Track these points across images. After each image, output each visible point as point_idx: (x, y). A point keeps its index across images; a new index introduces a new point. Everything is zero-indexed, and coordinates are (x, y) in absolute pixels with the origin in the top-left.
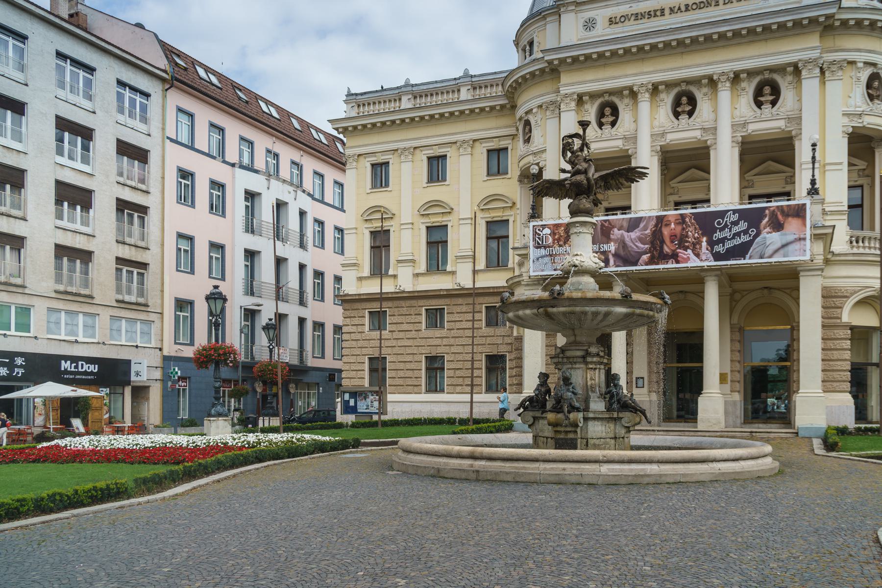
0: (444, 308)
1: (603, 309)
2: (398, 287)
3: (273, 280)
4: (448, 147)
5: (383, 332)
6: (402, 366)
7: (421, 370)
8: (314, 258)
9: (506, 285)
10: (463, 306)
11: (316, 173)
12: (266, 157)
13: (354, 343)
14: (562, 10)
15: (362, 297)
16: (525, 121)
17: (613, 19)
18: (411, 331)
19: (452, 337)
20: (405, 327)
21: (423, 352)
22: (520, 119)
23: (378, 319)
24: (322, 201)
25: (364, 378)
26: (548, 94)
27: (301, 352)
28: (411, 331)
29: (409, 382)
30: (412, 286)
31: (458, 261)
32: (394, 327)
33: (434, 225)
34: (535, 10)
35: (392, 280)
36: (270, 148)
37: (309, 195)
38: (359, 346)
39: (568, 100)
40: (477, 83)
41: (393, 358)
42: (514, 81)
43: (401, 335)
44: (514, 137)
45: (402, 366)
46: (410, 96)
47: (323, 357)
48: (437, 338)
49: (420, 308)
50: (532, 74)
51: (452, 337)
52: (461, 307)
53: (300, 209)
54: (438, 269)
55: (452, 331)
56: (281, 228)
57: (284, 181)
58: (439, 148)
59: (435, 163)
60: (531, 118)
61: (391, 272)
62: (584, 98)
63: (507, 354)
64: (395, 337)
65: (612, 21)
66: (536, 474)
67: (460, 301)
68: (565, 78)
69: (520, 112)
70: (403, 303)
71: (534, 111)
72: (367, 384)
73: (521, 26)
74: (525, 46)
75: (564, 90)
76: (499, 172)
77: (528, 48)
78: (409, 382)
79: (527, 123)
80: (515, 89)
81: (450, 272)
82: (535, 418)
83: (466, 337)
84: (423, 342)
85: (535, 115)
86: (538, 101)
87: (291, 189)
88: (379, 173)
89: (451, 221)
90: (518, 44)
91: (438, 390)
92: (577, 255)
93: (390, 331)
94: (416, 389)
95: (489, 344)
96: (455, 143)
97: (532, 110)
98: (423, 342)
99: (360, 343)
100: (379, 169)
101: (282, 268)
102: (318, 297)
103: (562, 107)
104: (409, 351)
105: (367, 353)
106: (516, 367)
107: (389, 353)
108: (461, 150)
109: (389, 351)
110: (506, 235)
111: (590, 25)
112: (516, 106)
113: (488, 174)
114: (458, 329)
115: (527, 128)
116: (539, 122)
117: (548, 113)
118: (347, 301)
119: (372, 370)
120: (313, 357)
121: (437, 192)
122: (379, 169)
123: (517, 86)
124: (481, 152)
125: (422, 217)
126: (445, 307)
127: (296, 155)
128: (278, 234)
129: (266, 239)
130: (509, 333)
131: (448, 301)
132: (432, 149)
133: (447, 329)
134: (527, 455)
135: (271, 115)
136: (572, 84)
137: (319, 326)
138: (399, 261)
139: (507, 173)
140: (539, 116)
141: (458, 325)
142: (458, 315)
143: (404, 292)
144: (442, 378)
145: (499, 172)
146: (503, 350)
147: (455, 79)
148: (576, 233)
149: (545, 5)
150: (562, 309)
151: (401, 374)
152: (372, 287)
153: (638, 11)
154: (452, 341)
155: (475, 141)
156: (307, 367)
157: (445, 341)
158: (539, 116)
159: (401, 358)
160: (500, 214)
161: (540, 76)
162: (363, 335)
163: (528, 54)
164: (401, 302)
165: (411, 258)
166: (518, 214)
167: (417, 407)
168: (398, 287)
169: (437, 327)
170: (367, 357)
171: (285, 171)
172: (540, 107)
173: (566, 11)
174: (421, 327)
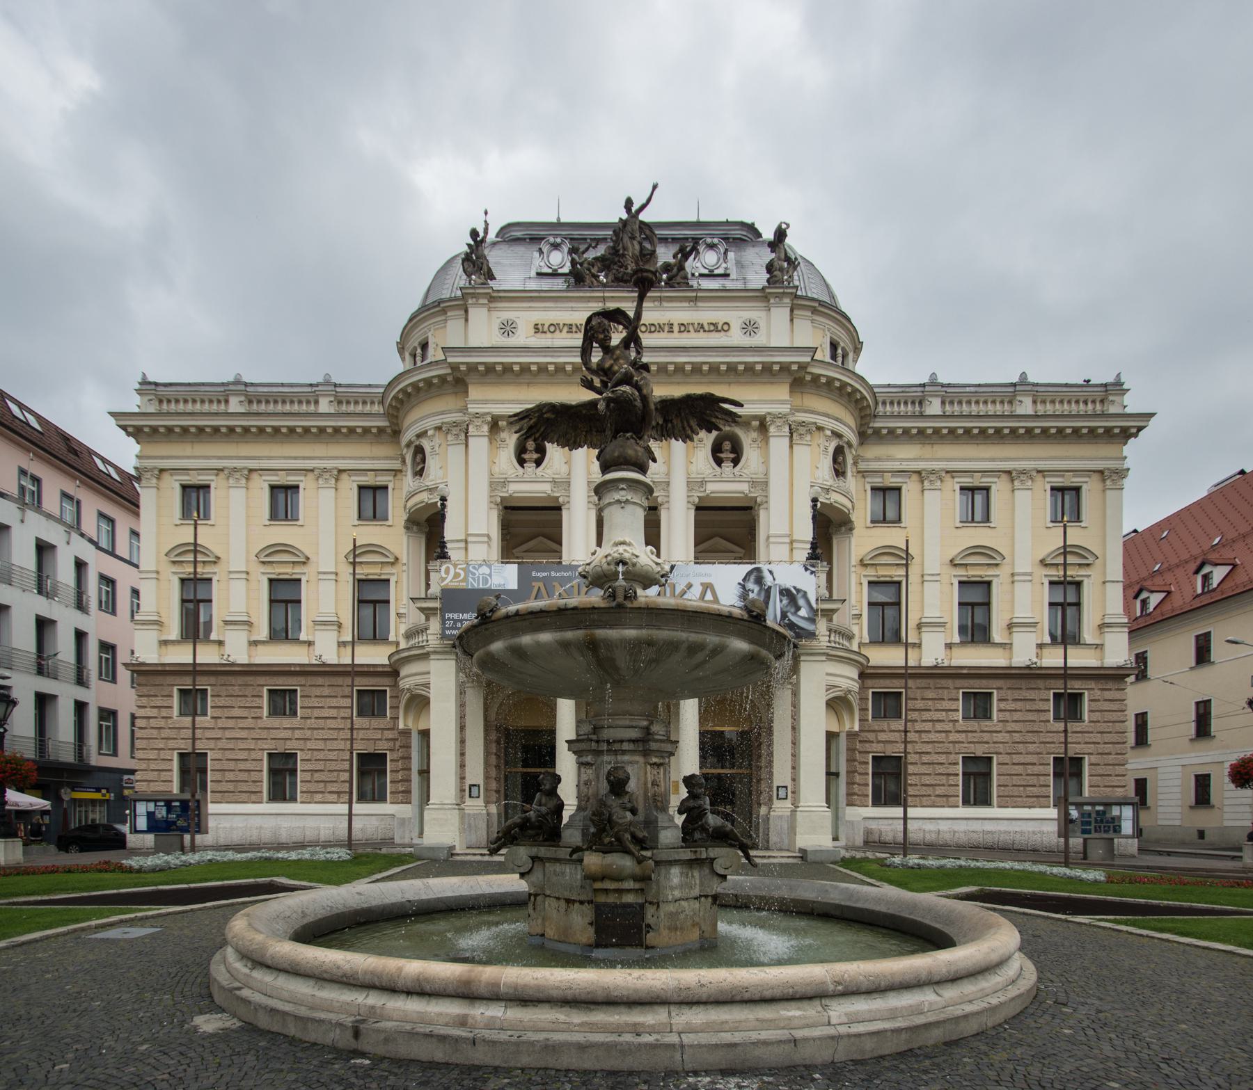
0: (296, 690)
1: (712, 639)
2: (226, 657)
3: (32, 647)
4: (301, 475)
5: (198, 719)
6: (231, 765)
7: (261, 771)
8: (98, 625)
9: (388, 663)
10: (323, 686)
11: (101, 515)
12: (19, 480)
13: (155, 732)
14: (470, 301)
15: (167, 668)
16: (416, 446)
17: (540, 327)
18: (246, 718)
19: (309, 729)
20: (236, 712)
21: (266, 747)
22: (408, 445)
23: (192, 700)
24: (112, 554)
25: (171, 781)
26: (450, 412)
27: (80, 746)
28: (246, 718)
29: (244, 787)
30: (246, 657)
31: (317, 627)
32: (218, 713)
33: (281, 577)
34: (428, 302)
35: (215, 647)
36: (25, 467)
37: (91, 541)
38: (163, 736)
39: (478, 422)
40: (343, 395)
41: (218, 755)
42: (401, 390)
43: (231, 723)
44: (396, 472)
45: (231, 765)
46: (242, 398)
47: (115, 754)
48: (285, 729)
49: (260, 688)
50: (428, 382)
51: (309, 729)
52: (322, 689)
53: (76, 557)
54: (287, 638)
55: (309, 721)
56: (45, 578)
57: (49, 516)
58: (287, 475)
59: (281, 497)
60: (425, 443)
61: (213, 636)
62: (500, 423)
63: (388, 752)
64: (220, 725)
65: (537, 329)
66: (671, 1046)
67: (320, 680)
68: (475, 392)
69: (408, 436)
70: (232, 679)
71: (430, 433)
72: (176, 790)
73: (411, 320)
74: (415, 348)
75: (473, 408)
76: (375, 516)
77: (419, 351)
78: (244, 787)
79: (420, 451)
80: (398, 409)
81: (305, 642)
82: (534, 859)
83: (329, 729)
84: (264, 734)
85: (431, 438)
86: (436, 421)
87: (61, 529)
88: (194, 503)
89: (307, 576)
90: (403, 348)
91: (288, 797)
92: (623, 543)
93: (212, 718)
94: (253, 797)
95: (362, 739)
96: (312, 471)
97: (426, 432)
98: (264, 734)
99: (165, 733)
100: (194, 495)
101: (47, 633)
102: (107, 676)
103: (471, 429)
104: (242, 745)
105: (176, 746)
106: (403, 769)
107: (212, 747)
108: (321, 481)
109: (212, 744)
110: (386, 598)
111: (508, 328)
112: (400, 432)
113: (360, 518)
114: (316, 718)
115: (419, 457)
116: (436, 448)
117: (450, 437)
118: (144, 674)
119: (184, 771)
120: (100, 754)
121: (282, 534)
122: (194, 495)
123: (405, 399)
124: (349, 489)
125: (262, 565)
126: (298, 688)
127: (71, 487)
128: (42, 587)
129: (20, 591)
130: (391, 726)
131: (301, 680)
132: (277, 475)
133: (302, 718)
134: (636, 991)
135: (28, 424)
136: (486, 402)
137: (108, 715)
138: (227, 623)
139: (387, 520)
140: (437, 441)
141: (317, 713)
142: (317, 699)
143: (233, 664)
144: (294, 784)
145: (375, 516)
146: (381, 747)
147: (311, 385)
148: (619, 502)
149: (443, 297)
150: (631, 633)
151: (231, 776)
152: (181, 655)
153: (573, 322)
154: (308, 733)
155: (340, 471)
156: (88, 766)
157: (298, 734)
158: (437, 441)
159: (229, 755)
160: (378, 571)
161: (439, 387)
162: (169, 721)
163: (419, 358)
164: (230, 678)
165: (246, 619)
166: (404, 571)
167: (257, 821)
168: (226, 657)
169: (285, 714)
170: (176, 752)
171: (51, 501)
172: (439, 428)
173: (476, 305)
174: (262, 713)
